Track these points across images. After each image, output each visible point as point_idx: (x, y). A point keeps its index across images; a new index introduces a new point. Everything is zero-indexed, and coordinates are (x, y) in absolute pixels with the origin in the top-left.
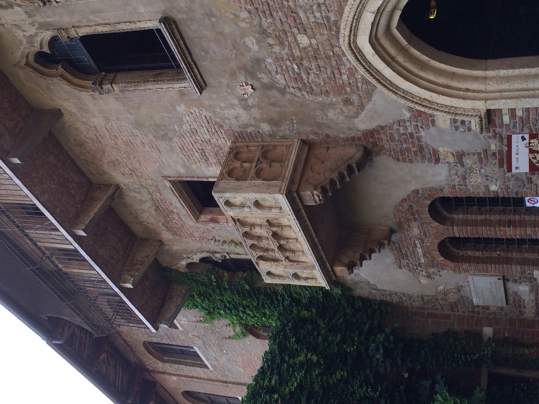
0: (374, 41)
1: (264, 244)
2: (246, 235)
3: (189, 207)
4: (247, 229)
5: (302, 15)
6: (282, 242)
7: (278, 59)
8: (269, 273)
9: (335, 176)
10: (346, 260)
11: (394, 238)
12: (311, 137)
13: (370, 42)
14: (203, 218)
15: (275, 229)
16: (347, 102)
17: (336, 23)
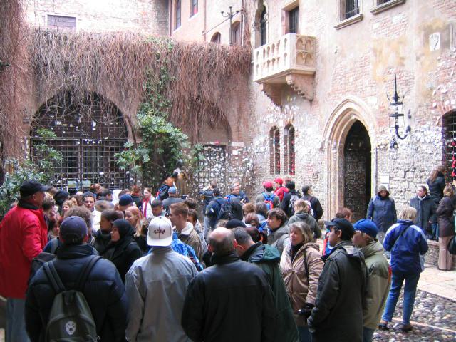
0: (349, 109)
1: (270, 52)
2: (273, 46)
3: (289, 6)
4: (276, 47)
5: (360, 80)
6: (271, 63)
7: (346, 67)
8: (258, 53)
9: (299, 89)
10: (266, 89)
11: (278, 108)
12: (317, 76)
13: (349, 108)
14: (284, 12)
15: (276, 60)
16: (329, 95)
17: (356, 95)
